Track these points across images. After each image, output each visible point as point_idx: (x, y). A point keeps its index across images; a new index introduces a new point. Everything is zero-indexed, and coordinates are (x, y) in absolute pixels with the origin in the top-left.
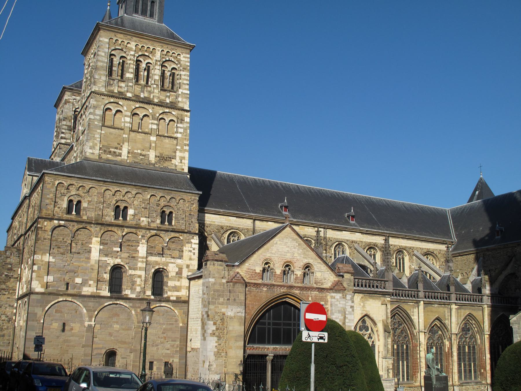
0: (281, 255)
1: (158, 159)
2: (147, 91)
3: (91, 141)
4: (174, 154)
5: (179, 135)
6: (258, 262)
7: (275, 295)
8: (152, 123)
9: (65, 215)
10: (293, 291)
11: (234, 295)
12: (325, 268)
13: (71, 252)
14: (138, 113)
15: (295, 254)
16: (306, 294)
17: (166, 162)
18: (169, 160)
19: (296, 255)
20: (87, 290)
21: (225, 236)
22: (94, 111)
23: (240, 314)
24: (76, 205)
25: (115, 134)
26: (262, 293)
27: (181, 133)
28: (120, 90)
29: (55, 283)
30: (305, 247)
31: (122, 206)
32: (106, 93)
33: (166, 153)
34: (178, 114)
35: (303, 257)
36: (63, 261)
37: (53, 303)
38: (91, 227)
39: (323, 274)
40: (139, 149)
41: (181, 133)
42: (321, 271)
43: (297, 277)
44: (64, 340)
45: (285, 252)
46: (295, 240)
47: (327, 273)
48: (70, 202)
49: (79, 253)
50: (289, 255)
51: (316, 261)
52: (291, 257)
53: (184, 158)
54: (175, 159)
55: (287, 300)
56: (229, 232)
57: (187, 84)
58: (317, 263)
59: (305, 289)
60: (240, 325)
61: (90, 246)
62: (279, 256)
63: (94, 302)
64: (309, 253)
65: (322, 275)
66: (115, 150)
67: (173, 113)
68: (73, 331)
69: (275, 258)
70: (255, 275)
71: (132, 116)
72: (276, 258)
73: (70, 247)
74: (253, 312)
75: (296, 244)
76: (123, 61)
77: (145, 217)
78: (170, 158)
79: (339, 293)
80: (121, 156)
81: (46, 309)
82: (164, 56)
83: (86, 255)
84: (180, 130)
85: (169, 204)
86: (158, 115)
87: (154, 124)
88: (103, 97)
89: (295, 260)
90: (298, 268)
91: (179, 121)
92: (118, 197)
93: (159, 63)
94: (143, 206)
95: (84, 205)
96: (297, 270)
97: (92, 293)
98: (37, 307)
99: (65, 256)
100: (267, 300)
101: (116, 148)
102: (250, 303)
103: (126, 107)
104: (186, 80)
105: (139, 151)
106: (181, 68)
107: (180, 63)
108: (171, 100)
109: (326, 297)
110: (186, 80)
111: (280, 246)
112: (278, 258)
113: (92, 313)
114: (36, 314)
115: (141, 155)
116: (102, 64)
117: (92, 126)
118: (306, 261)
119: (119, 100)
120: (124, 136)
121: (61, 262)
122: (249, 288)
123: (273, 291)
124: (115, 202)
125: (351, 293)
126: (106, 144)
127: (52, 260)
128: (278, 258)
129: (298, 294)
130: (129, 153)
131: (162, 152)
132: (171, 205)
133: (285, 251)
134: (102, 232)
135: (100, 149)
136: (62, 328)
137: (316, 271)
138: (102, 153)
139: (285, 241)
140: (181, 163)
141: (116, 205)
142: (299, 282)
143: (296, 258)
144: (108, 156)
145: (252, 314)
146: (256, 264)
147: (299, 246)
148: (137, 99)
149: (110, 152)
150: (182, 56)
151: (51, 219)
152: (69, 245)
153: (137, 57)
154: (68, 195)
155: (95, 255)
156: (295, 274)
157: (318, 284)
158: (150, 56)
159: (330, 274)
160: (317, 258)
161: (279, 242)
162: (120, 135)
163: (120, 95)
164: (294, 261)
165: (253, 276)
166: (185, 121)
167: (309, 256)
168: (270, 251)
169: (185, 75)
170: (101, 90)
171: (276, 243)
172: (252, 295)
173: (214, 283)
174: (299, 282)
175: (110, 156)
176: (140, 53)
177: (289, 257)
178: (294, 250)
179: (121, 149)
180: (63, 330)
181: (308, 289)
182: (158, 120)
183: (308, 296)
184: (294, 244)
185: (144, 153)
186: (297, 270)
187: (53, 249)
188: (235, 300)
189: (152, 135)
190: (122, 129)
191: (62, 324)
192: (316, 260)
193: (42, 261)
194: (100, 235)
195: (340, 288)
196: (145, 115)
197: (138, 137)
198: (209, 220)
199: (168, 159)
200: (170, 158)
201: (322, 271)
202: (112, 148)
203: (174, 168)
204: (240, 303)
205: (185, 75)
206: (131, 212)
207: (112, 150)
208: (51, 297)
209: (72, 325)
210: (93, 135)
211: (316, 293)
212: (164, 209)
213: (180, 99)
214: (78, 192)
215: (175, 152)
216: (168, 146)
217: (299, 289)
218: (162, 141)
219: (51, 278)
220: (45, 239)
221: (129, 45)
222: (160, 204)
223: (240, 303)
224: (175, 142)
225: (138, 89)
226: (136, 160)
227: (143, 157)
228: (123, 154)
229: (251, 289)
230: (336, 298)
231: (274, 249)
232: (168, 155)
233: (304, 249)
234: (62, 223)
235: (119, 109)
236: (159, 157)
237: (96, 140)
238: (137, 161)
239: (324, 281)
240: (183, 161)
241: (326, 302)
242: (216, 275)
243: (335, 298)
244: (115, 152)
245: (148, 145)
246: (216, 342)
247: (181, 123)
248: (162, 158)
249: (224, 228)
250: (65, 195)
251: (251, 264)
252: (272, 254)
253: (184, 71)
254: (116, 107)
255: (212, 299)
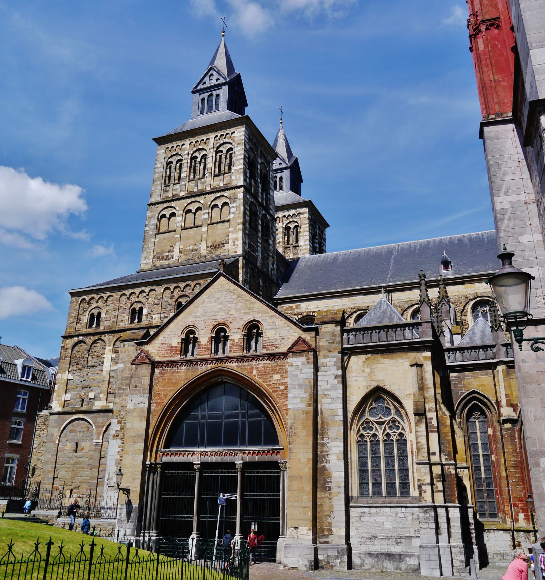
0: (209, 316)
1: (210, 249)
2: (201, 184)
3: (145, 252)
4: (227, 238)
5: (231, 216)
6: (176, 333)
7: (199, 373)
8: (204, 214)
9: (85, 330)
10: (226, 364)
11: (136, 380)
12: (282, 322)
13: (87, 367)
14: (191, 208)
15: (231, 311)
16: (249, 365)
17: (219, 249)
18: (221, 247)
19: (232, 312)
20: (98, 405)
21: (350, 322)
22: (150, 222)
23: (141, 406)
24: (96, 317)
25: (168, 238)
26: (179, 374)
27: (233, 213)
28: (175, 192)
29: (72, 400)
30: (247, 298)
31: (137, 306)
32: (161, 201)
33: (218, 240)
34: (230, 194)
35: (244, 313)
36: (80, 377)
37: (68, 421)
38: (105, 336)
39: (278, 332)
40: (191, 245)
41: (233, 213)
42: (275, 327)
43: (233, 344)
44: (75, 462)
45: (215, 312)
46: (231, 292)
47: (287, 328)
48: (92, 316)
49: (93, 366)
50: (220, 314)
51: (267, 315)
52: (224, 317)
53: (237, 239)
54: (228, 243)
55: (224, 380)
56: (355, 315)
57: (242, 158)
58: (267, 318)
59: (245, 359)
60: (141, 421)
61: (104, 356)
62: (206, 318)
63: (102, 417)
64: (255, 306)
65: (276, 334)
66: (168, 254)
67: (225, 194)
68: (83, 451)
69: (200, 322)
70: (171, 350)
71: (184, 214)
72: (202, 321)
73: (86, 361)
74: (165, 401)
75: (233, 296)
76: (181, 165)
77: (158, 314)
78: (223, 244)
79: (300, 356)
80: (173, 258)
81: (62, 429)
82: (218, 141)
83: (100, 367)
84: (232, 210)
85: (184, 293)
86: (209, 203)
87: (206, 213)
88: (157, 206)
89: (231, 319)
90: (236, 330)
91: (232, 201)
92: (134, 299)
93: (212, 150)
94: (156, 302)
95: (103, 315)
96: (234, 333)
97: (102, 407)
98: (54, 427)
99: (82, 371)
100: (186, 382)
101: (169, 252)
102: (162, 388)
103: (179, 206)
104: (240, 155)
105: (191, 247)
106: (236, 145)
107: (234, 141)
108: (225, 183)
109: (285, 366)
110: (240, 155)
111: (209, 305)
112: (205, 321)
113: (101, 429)
114: (53, 435)
115: (193, 250)
116: (158, 175)
117: (146, 238)
118: (249, 318)
119: (171, 203)
120: (176, 236)
121: (79, 378)
122: (162, 368)
123: (195, 369)
124: (130, 305)
125: (336, 353)
126: (159, 250)
127: (71, 377)
128: (205, 321)
129: (235, 368)
130: (180, 252)
131: (214, 240)
132: (187, 294)
133: (216, 310)
134: (115, 339)
135: (154, 257)
136: (75, 448)
137: (266, 329)
138: (155, 261)
139: (216, 296)
140: (234, 245)
141: (131, 308)
142: (237, 350)
143: (232, 316)
144: (161, 262)
145: (164, 404)
146: (173, 335)
147: (238, 299)
148: (192, 195)
149: (163, 257)
150: (236, 132)
151: (71, 337)
152: (86, 359)
153: (192, 154)
154: (89, 310)
155: (107, 365)
156: (231, 340)
157: (270, 348)
158: (205, 147)
159: (291, 329)
160: (268, 309)
161: (207, 300)
162: (173, 237)
163: (173, 197)
164: (229, 322)
165: (168, 352)
166: (238, 198)
167: (254, 310)
168: (193, 315)
169: (239, 151)
170: (156, 200)
171: (203, 302)
172: (164, 378)
173: (122, 369)
174: (237, 350)
175: (163, 262)
176: (195, 149)
177: (221, 317)
178: (229, 306)
179: (173, 251)
180: (76, 451)
181: (250, 359)
182: (211, 208)
183: (252, 369)
184: (229, 298)
185: (195, 247)
186: (234, 333)
187: (73, 366)
188: (136, 387)
189: (204, 226)
190: (175, 231)
191: (75, 444)
192: (266, 313)
193: (62, 380)
194: (112, 344)
195: (301, 349)
196: (199, 209)
197: (190, 233)
198: (327, 305)
199: (220, 246)
200: (223, 244)
201: (277, 328)
202: (165, 252)
203: (226, 253)
204: (143, 390)
205: (239, 151)
206: (145, 311)
207: (165, 254)
208: (67, 416)
209: (83, 444)
210: (147, 246)
211: (265, 362)
212: (180, 300)
213: (233, 178)
214: (97, 304)
215: (228, 236)
216: (220, 232)
217: (235, 360)
218: (214, 228)
219: (68, 397)
220: (66, 357)
221: (184, 147)
222: (174, 296)
223: (143, 390)
224: (227, 224)
225: (192, 185)
226: (188, 257)
227: (195, 252)
228: (174, 256)
229: (164, 370)
230: (294, 364)
231: (200, 310)
232: (221, 242)
233: (246, 301)
234: (81, 338)
235: (172, 212)
236: (211, 246)
237: (150, 249)
238: (189, 257)
239: (280, 343)
240: (236, 243)
241: (284, 375)
242: (126, 359)
243: (292, 365)
244: (167, 256)
245: (200, 237)
246: (119, 447)
247: (234, 202)
248: (215, 247)
249: (348, 311)
250: (87, 311)
251: (166, 336)
252: (197, 317)
253: (237, 147)
254: (170, 210)
255: (118, 390)
